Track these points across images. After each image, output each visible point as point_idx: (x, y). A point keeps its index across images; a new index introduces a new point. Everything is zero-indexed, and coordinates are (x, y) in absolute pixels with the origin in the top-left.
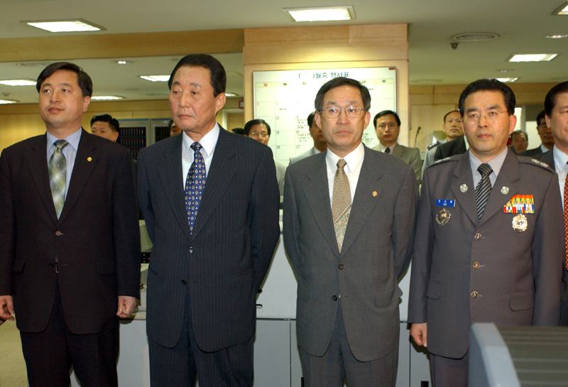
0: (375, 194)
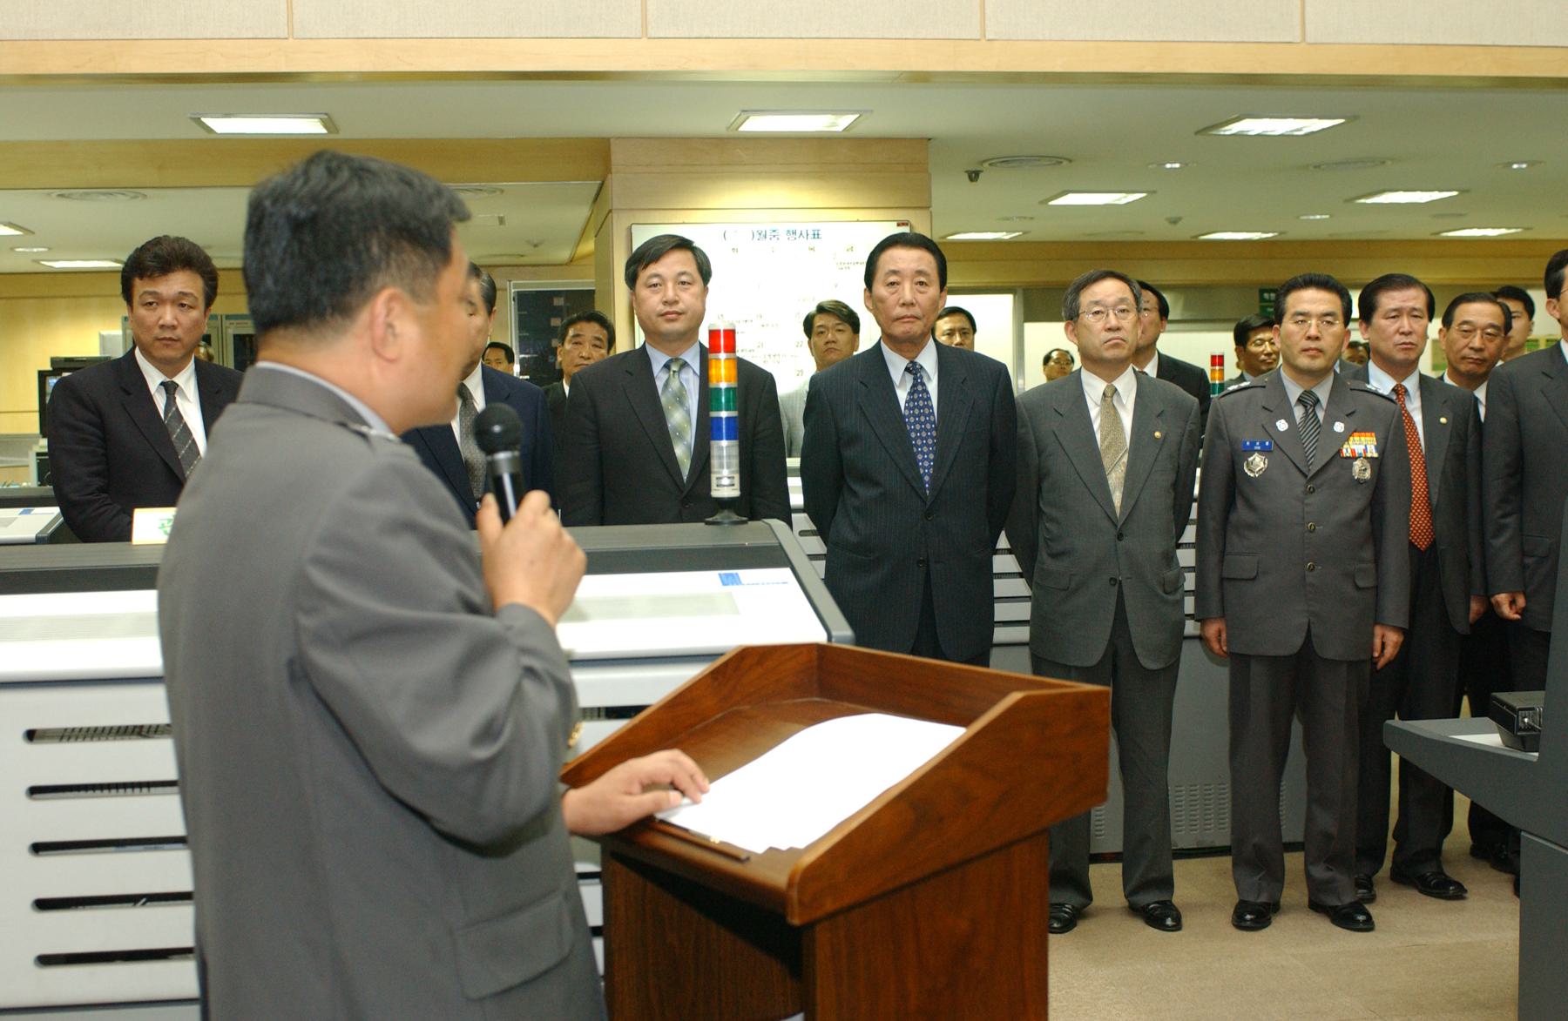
0: (1157, 434)
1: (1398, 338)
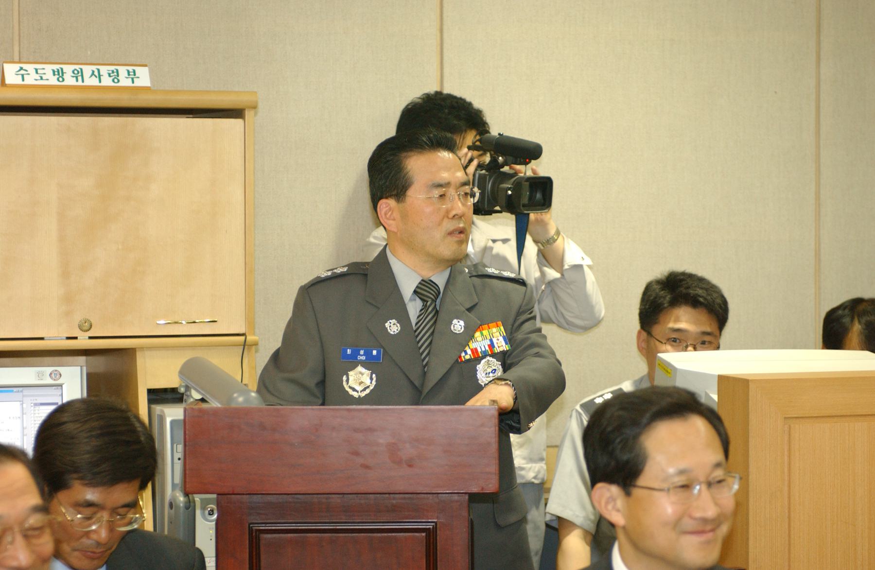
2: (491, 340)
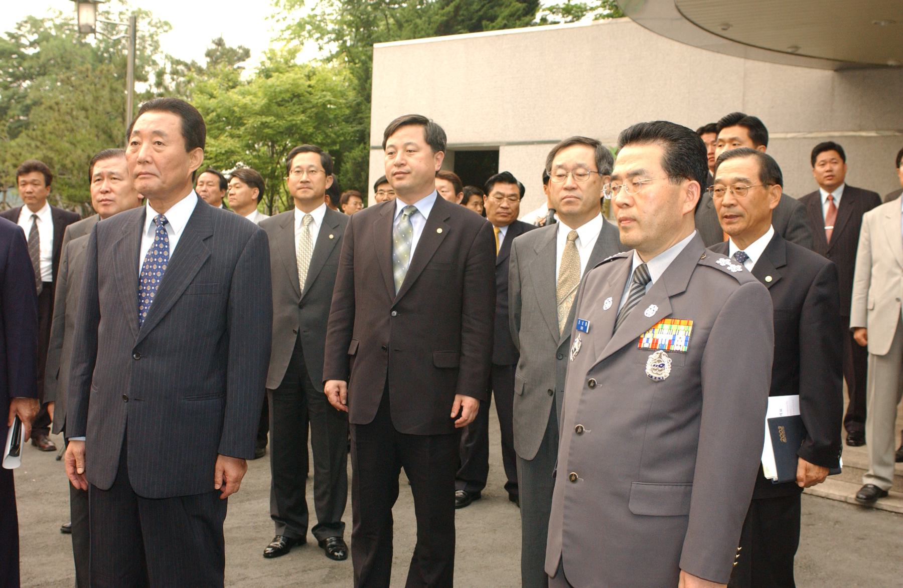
1: (564, 193)
2: (674, 336)
